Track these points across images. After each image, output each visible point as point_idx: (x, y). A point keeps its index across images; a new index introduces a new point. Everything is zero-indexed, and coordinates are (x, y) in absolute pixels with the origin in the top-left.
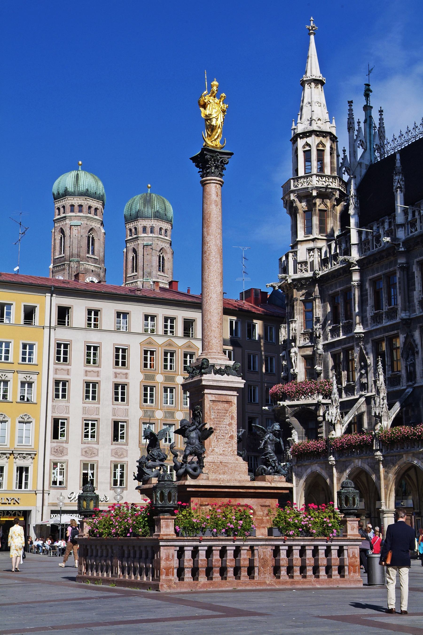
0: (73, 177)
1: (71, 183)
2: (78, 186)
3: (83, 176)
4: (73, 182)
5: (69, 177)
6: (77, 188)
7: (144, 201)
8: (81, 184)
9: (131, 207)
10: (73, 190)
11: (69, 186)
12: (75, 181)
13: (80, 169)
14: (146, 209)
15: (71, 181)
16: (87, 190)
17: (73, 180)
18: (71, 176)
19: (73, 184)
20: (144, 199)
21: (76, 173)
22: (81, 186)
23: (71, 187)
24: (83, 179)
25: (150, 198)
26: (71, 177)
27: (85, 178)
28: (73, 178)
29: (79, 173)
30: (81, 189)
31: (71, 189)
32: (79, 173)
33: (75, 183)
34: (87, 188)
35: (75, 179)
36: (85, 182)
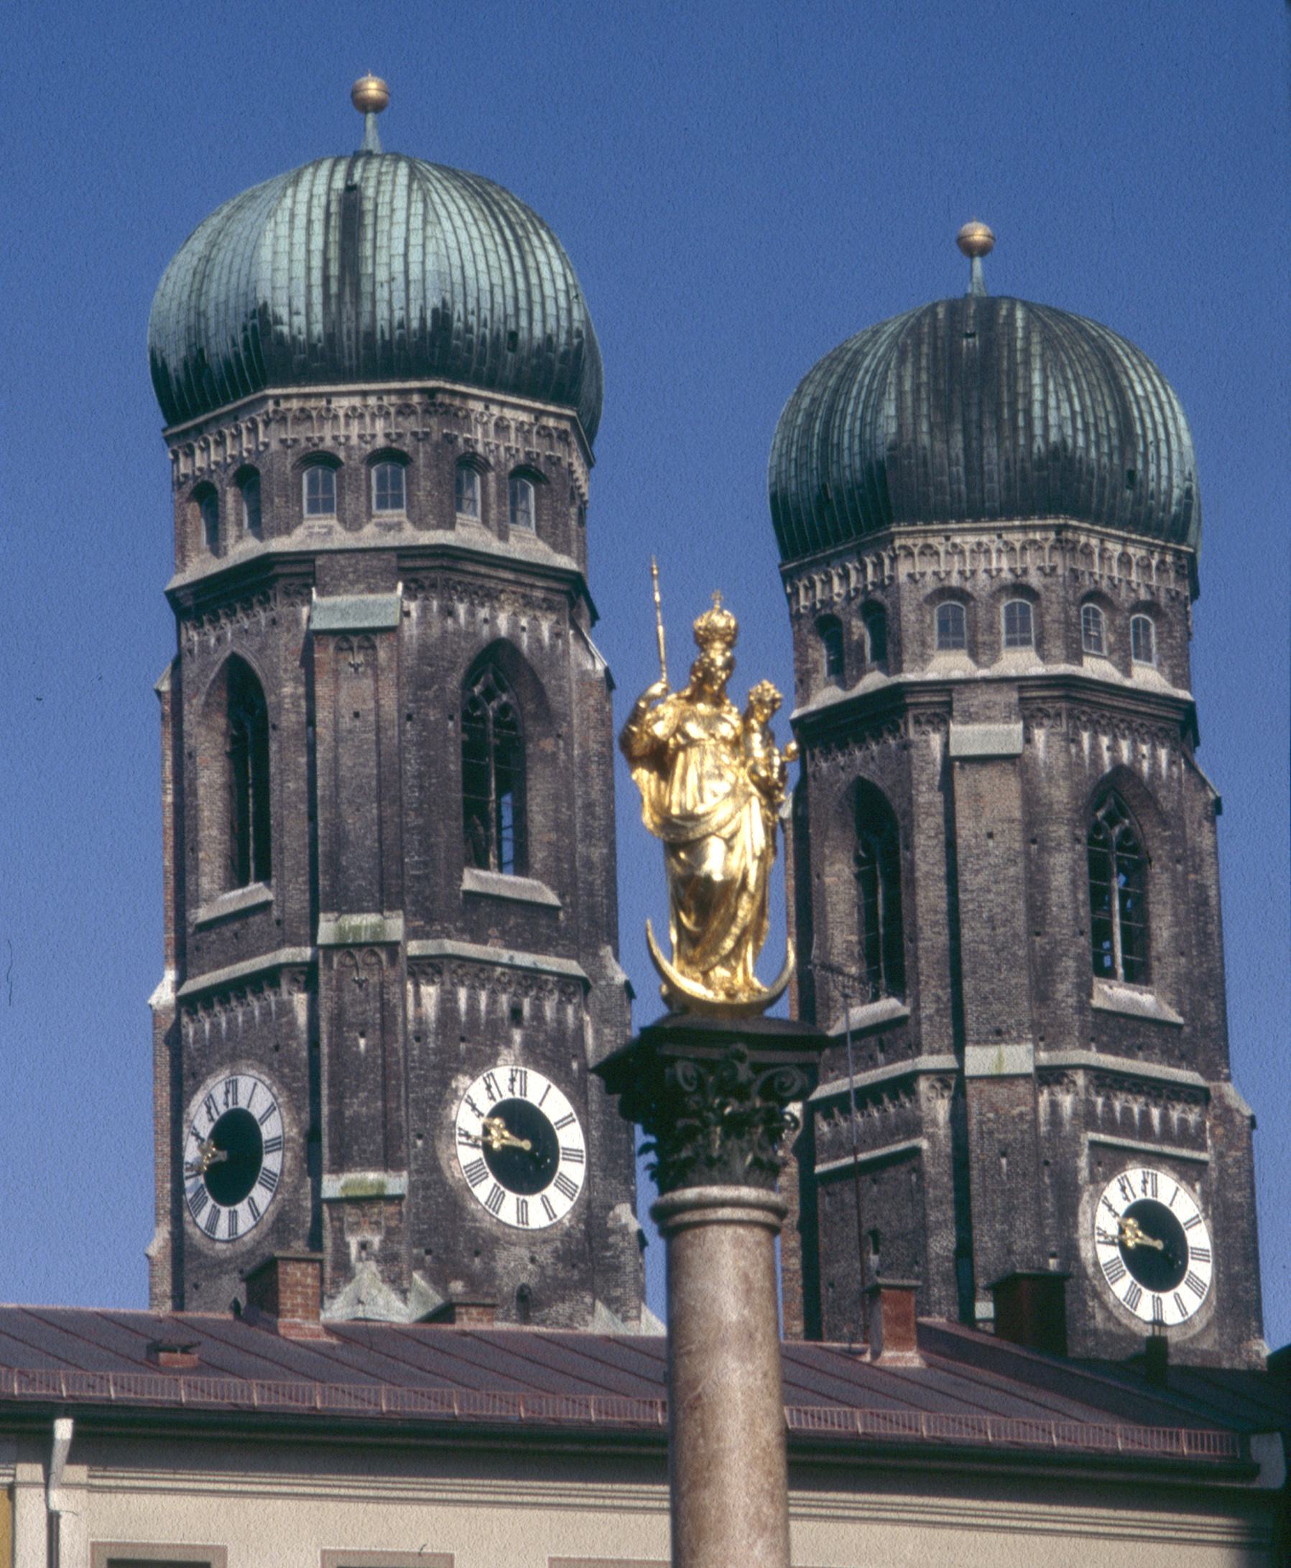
0: (318, 214)
1: (299, 270)
2: (357, 294)
3: (400, 203)
4: (317, 262)
5: (283, 216)
6: (348, 309)
7: (935, 377)
8: (382, 275)
9: (827, 424)
10: (318, 328)
11: (282, 297)
12: (334, 252)
13: (372, 141)
14: (958, 441)
15: (300, 253)
16: (442, 317)
17: (317, 242)
18: (301, 209)
19: (317, 276)
20: (934, 360)
21: (339, 184)
22: (382, 293)
23: (300, 304)
24: (399, 232)
25: (989, 346)
26: (301, 221)
27: (416, 222)
28: (318, 228)
29: (368, 175)
30: (382, 311)
31: (300, 321)
32: (368, 175)
33: (334, 270)
34: (434, 301)
35: (334, 236)
36: (415, 255)
